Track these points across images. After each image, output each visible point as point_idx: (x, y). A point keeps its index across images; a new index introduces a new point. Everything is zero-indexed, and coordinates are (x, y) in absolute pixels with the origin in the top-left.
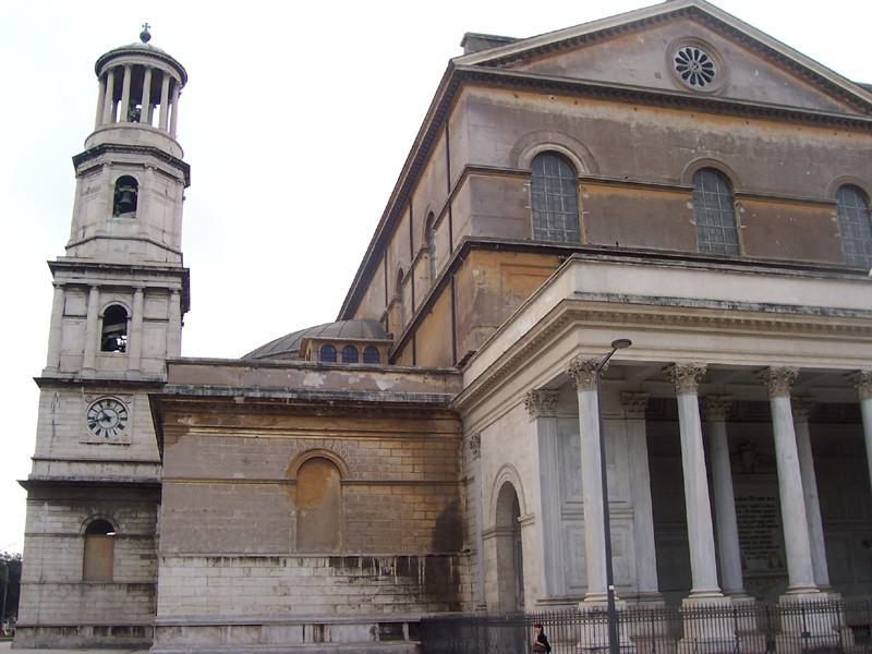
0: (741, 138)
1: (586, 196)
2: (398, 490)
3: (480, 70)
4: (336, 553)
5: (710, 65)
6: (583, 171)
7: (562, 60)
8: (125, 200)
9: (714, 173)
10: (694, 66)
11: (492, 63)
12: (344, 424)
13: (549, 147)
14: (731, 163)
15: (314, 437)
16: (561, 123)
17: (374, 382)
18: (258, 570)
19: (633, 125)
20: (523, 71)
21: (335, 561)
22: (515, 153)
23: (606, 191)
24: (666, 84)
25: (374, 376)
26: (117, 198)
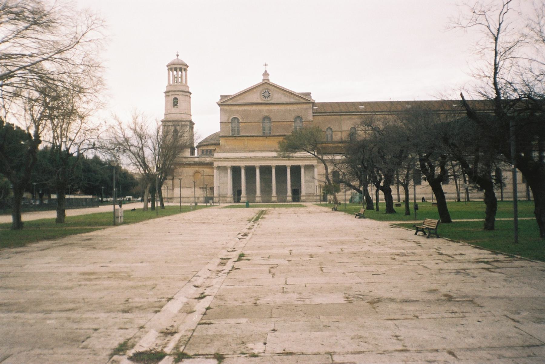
0: (274, 109)
1: (241, 125)
2: (210, 177)
3: (221, 104)
4: (201, 186)
5: (270, 93)
6: (241, 120)
7: (238, 98)
8: (175, 103)
9: (267, 118)
10: (266, 94)
11: (224, 102)
12: (201, 166)
13: (234, 117)
14: (271, 116)
15: (196, 168)
16: (237, 111)
17: (206, 159)
18: (189, 189)
19: (251, 109)
20: (230, 102)
21: (200, 188)
22: (229, 118)
23: (244, 124)
24: (260, 101)
25: (206, 158)
26: (174, 103)
